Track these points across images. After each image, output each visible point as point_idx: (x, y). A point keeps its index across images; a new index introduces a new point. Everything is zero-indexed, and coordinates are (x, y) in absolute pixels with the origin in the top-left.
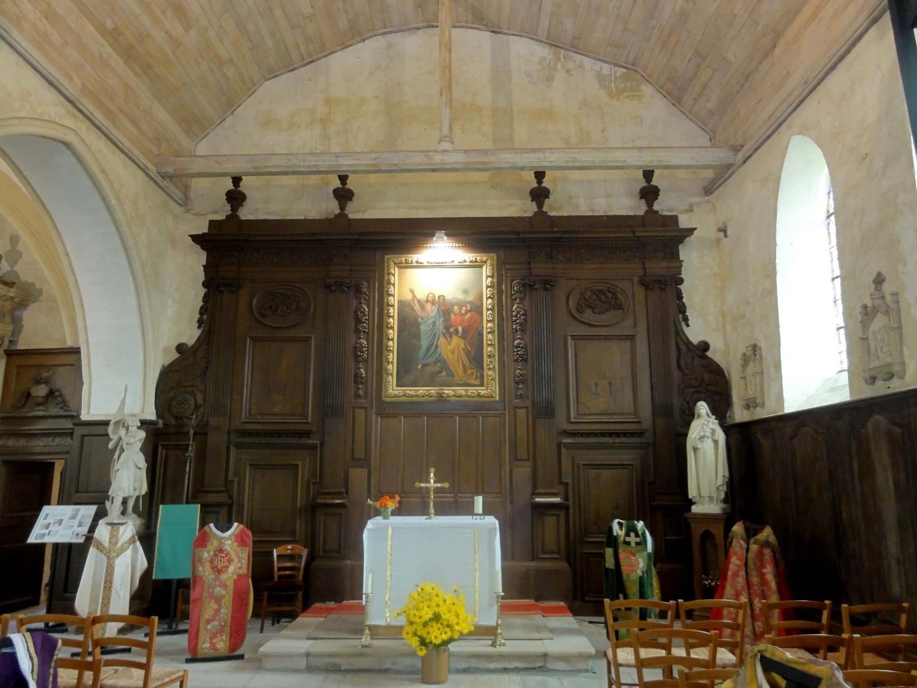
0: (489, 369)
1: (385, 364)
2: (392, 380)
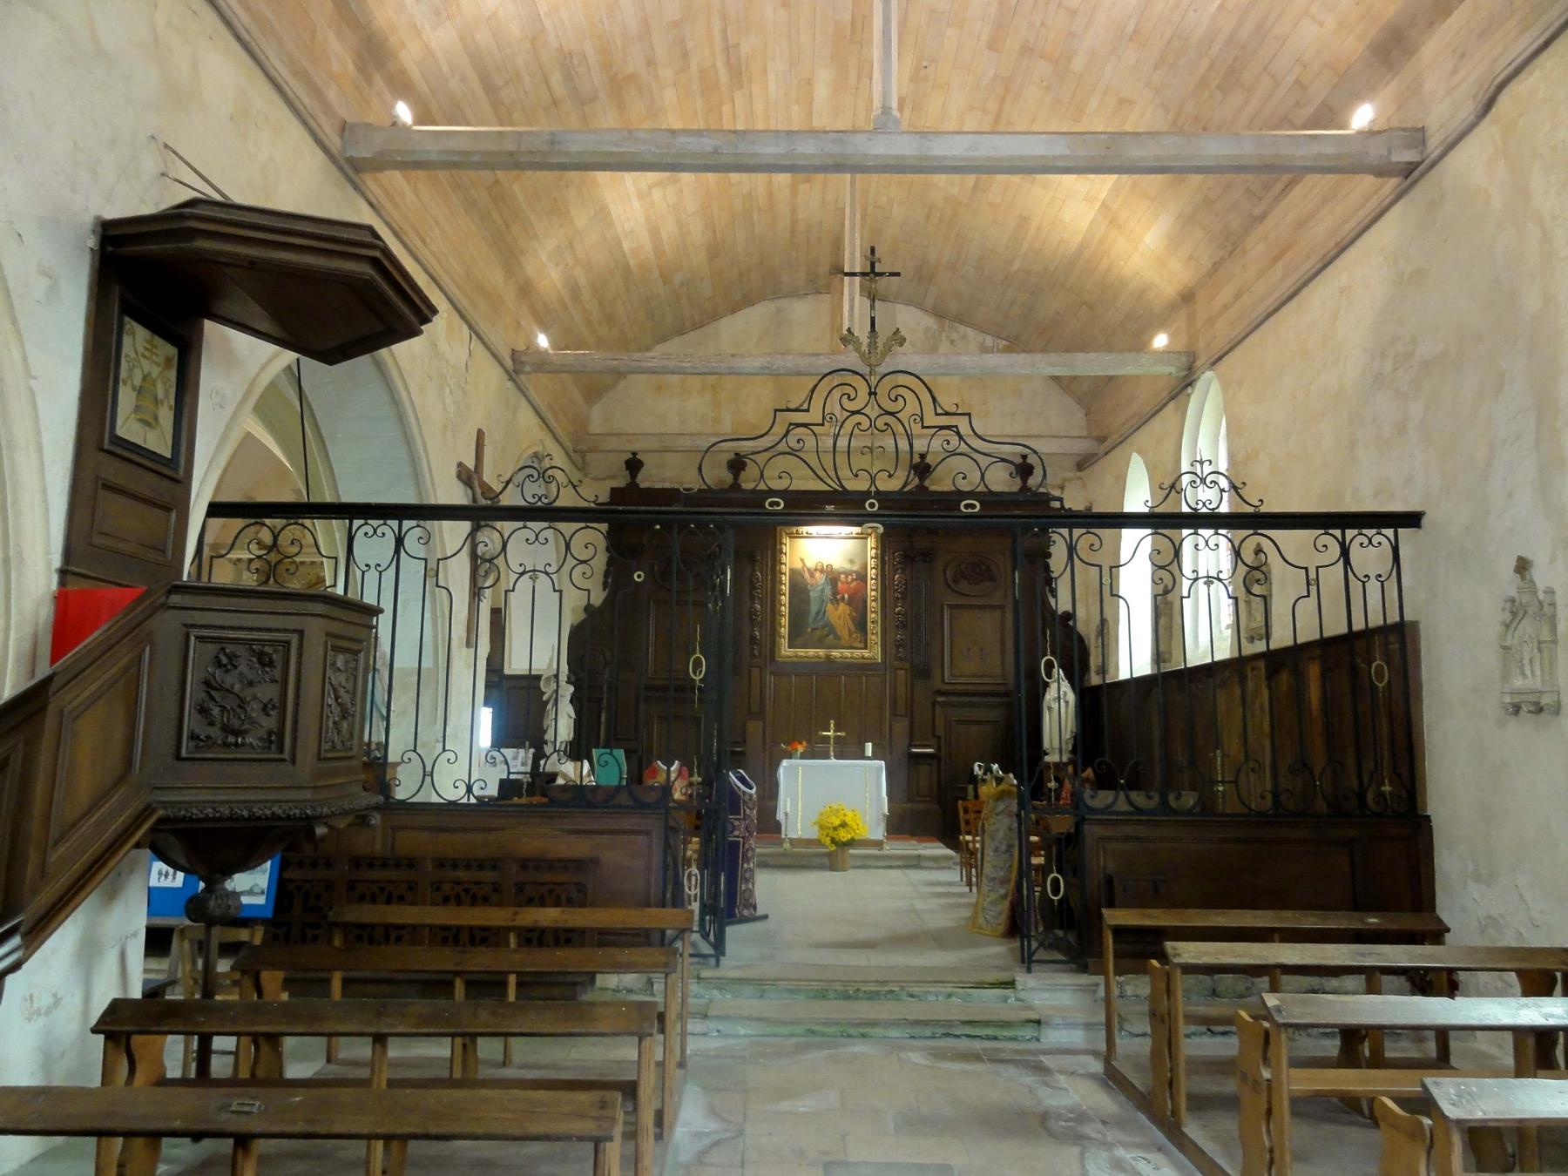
2: (784, 642)
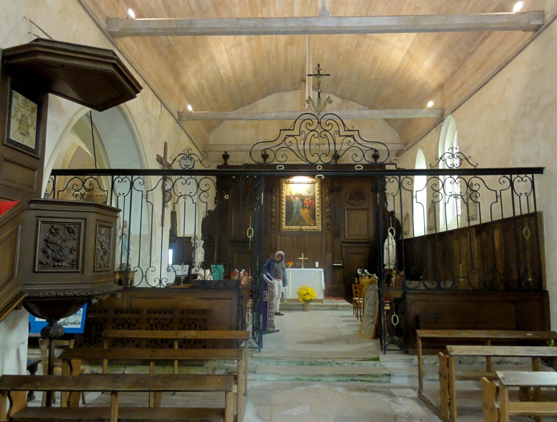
2: (284, 224)
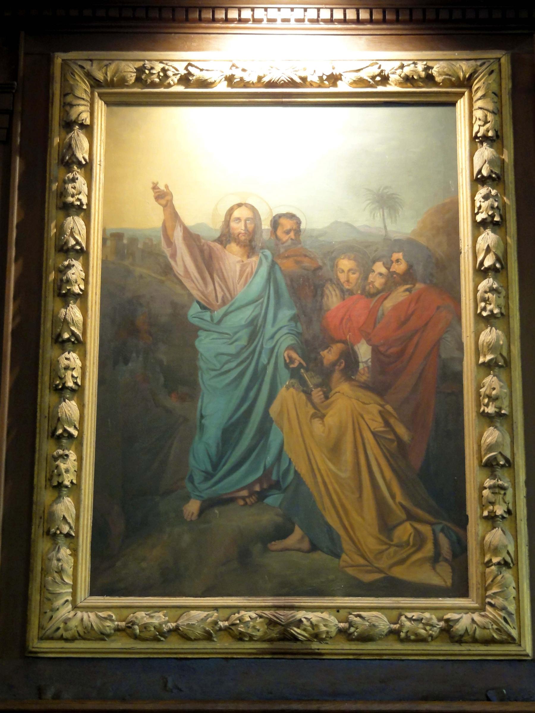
0: (492, 519)
1: (45, 496)
2: (70, 567)
